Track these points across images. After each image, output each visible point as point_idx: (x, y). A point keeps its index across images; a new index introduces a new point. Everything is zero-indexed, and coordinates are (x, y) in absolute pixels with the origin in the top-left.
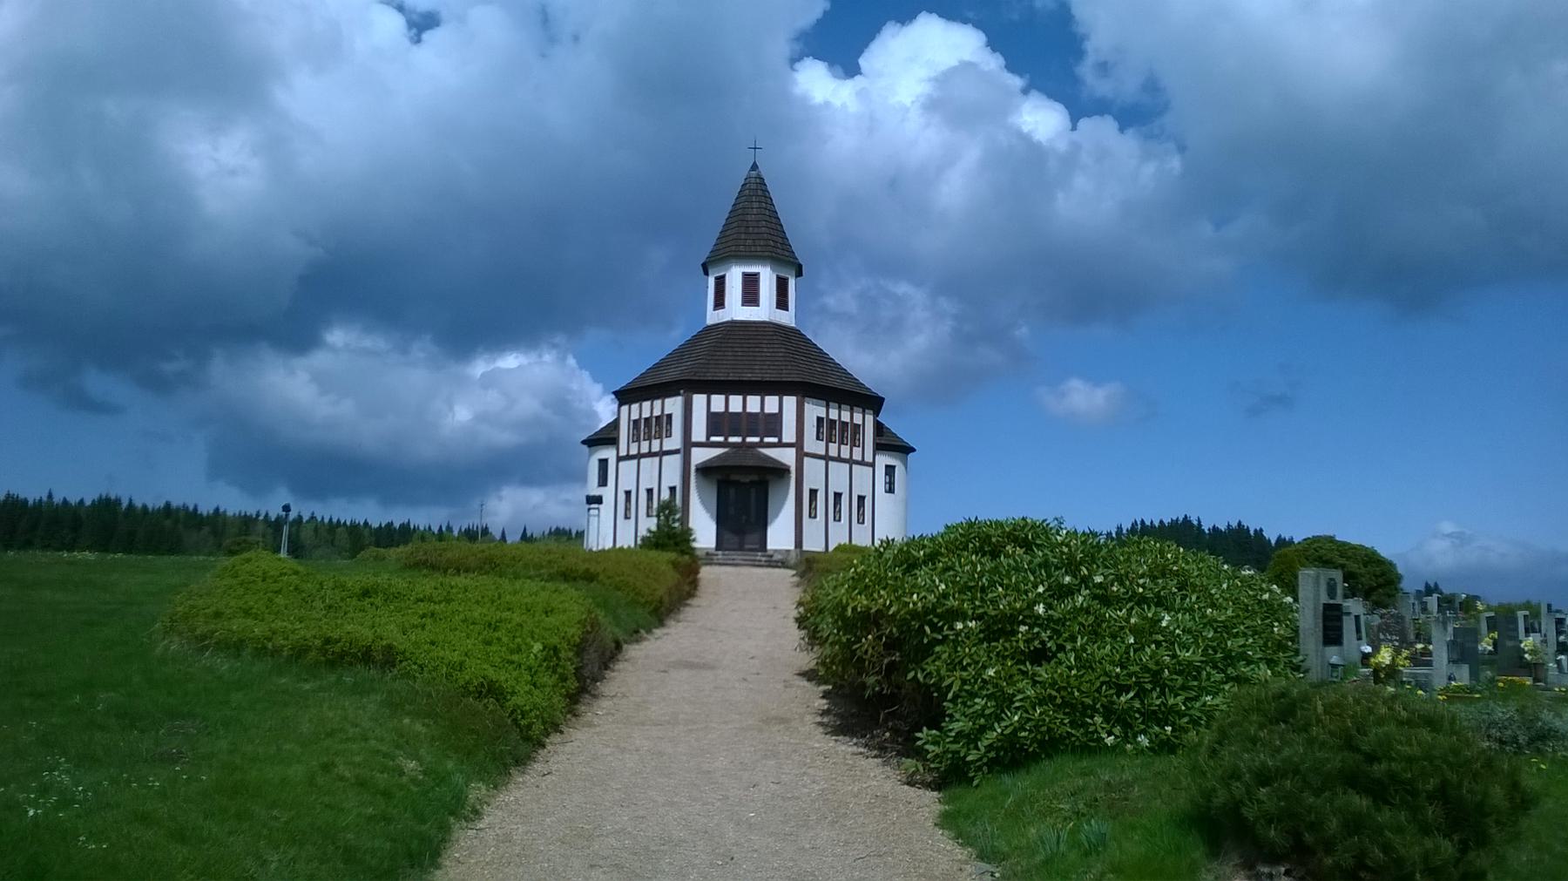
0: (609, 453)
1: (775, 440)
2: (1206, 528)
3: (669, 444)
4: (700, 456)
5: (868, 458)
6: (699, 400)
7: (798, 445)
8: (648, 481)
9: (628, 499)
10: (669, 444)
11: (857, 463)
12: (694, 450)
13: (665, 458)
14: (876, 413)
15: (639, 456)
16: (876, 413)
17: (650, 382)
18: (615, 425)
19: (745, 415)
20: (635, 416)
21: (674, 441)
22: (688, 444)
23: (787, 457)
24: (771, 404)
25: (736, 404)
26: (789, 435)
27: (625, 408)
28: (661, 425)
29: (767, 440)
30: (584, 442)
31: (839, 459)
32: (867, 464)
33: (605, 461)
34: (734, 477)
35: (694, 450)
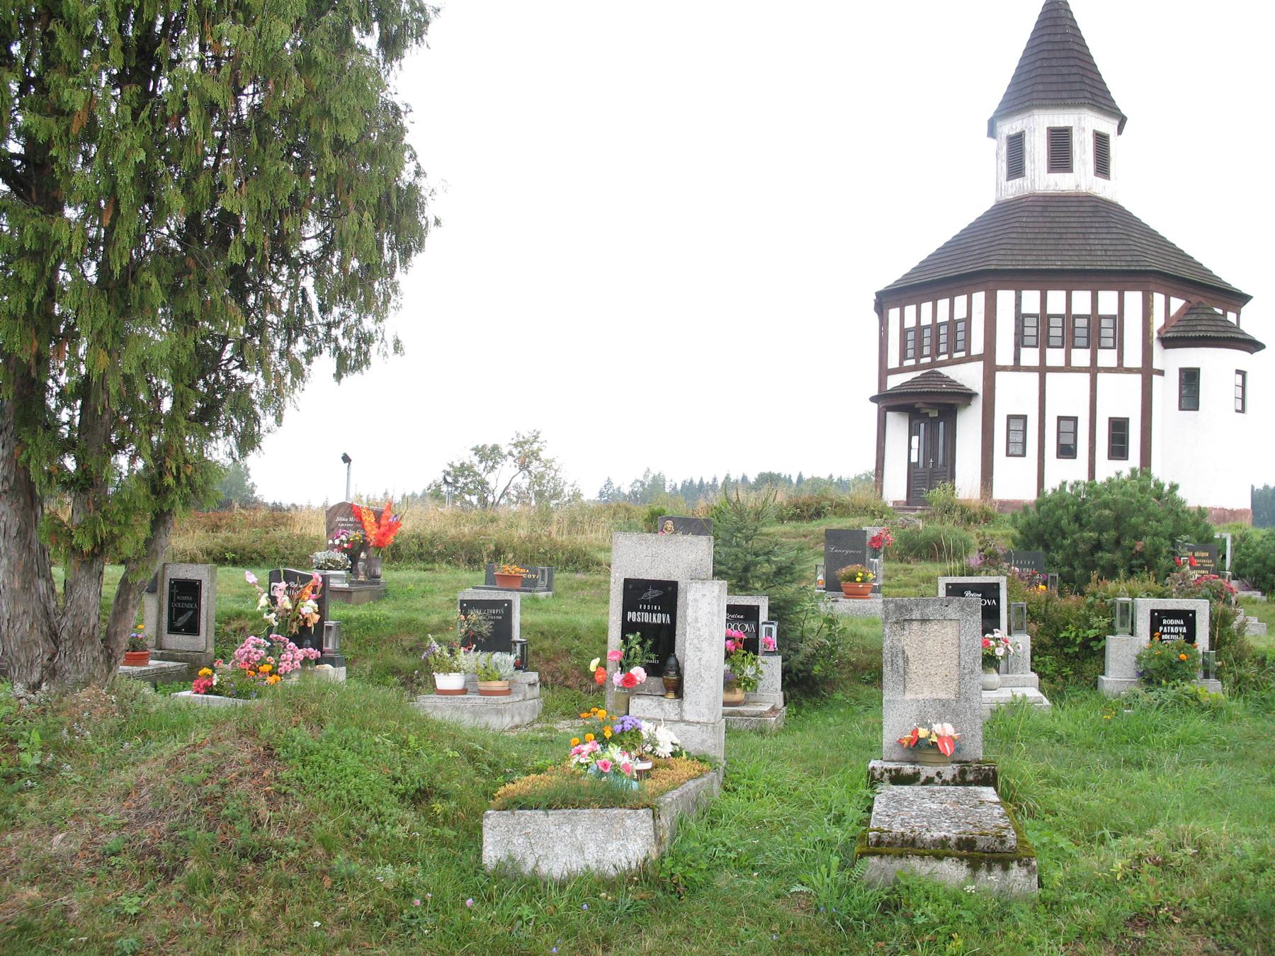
6: (1005, 298)
17: (923, 279)
24: (1108, 301)
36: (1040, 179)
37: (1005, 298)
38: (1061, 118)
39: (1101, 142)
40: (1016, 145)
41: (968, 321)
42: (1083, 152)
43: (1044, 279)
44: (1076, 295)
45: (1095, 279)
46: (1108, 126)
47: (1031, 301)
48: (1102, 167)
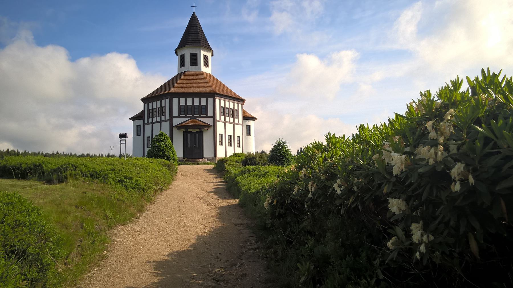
0: (140, 122)
4: (176, 122)
5: (240, 122)
6: (175, 100)
7: (214, 117)
9: (148, 141)
11: (237, 124)
12: (174, 119)
14: (242, 105)
15: (152, 123)
16: (242, 105)
18: (143, 112)
19: (193, 106)
22: (171, 117)
23: (209, 121)
24: (203, 102)
25: (189, 102)
26: (210, 113)
27: (146, 105)
28: (161, 111)
30: (130, 119)
32: (240, 125)
34: (190, 130)
37: (175, 100)
39: (206, 57)
41: (165, 106)
43: (186, 95)
45: (200, 95)
47: (182, 101)
48: (206, 64)
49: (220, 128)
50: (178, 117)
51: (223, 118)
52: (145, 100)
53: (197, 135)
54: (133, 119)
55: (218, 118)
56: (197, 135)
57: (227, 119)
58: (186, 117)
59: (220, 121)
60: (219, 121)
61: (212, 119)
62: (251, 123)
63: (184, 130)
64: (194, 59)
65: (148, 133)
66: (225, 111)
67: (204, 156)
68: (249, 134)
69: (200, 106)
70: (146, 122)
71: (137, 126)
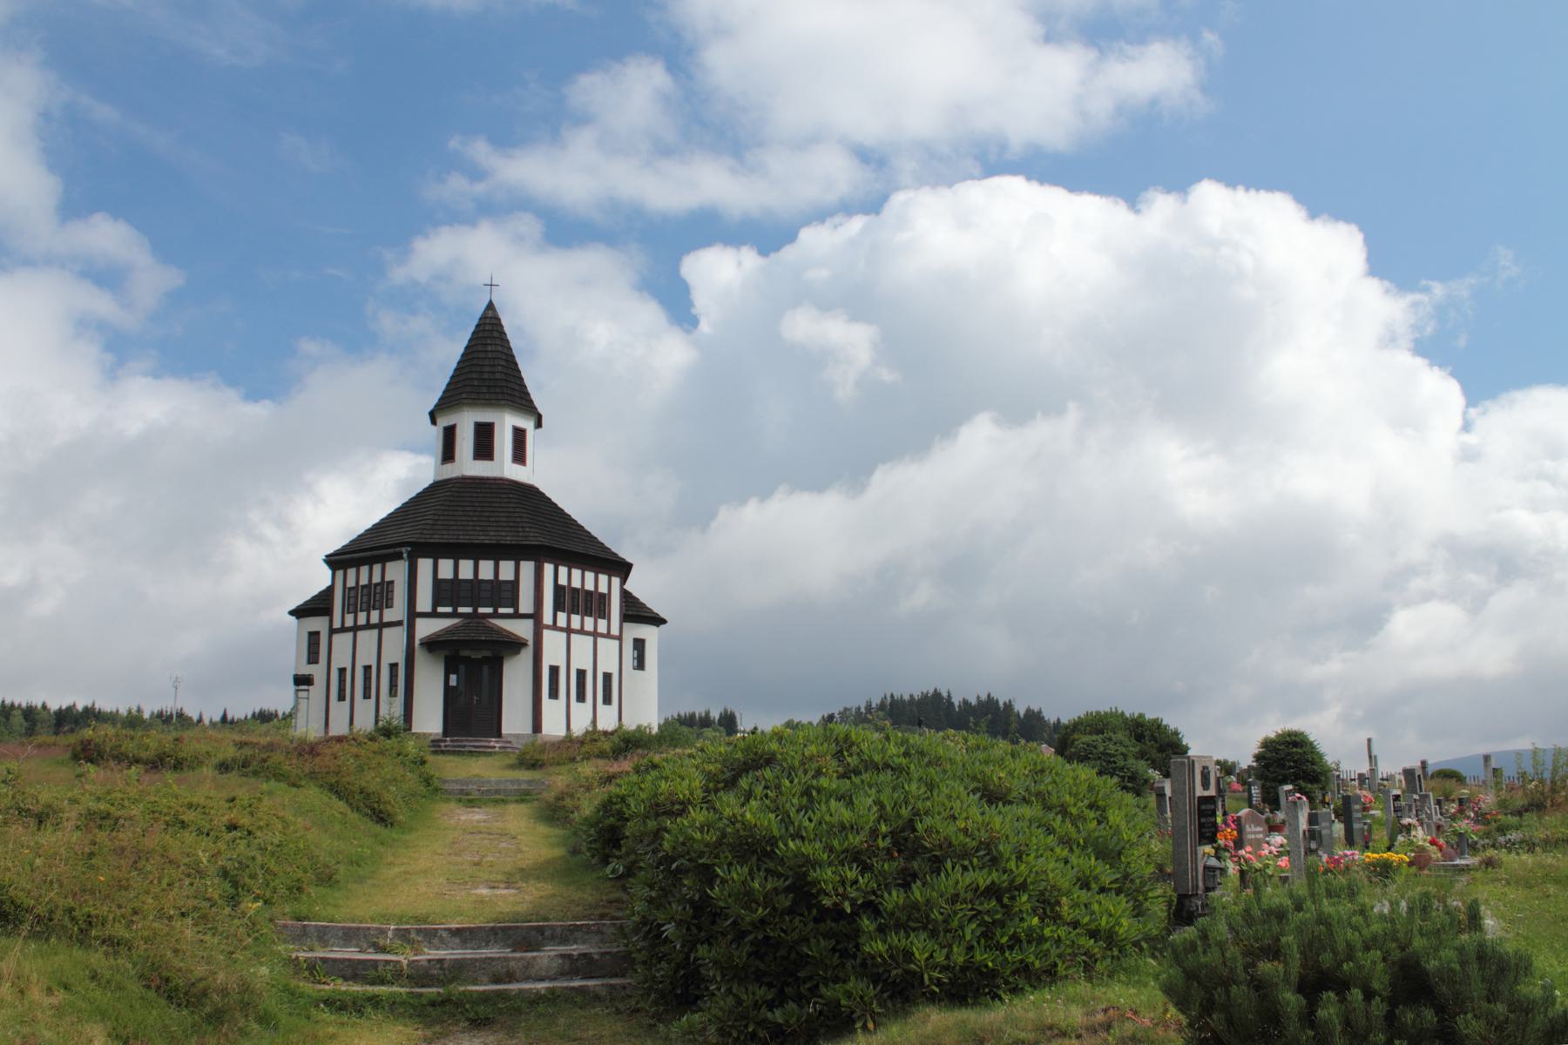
0: (318, 624)
1: (510, 610)
2: (956, 701)
3: (389, 615)
4: (425, 628)
5: (615, 631)
6: (425, 565)
7: (536, 616)
8: (366, 656)
10: (389, 615)
11: (603, 636)
12: (420, 622)
13: (386, 631)
15: (355, 629)
18: (329, 592)
19: (476, 582)
20: (351, 583)
21: (397, 612)
22: (413, 615)
23: (523, 629)
24: (507, 570)
25: (466, 570)
26: (526, 605)
27: (340, 574)
29: (501, 610)
30: (292, 613)
31: (582, 632)
32: (614, 638)
33: (317, 633)
34: (465, 653)
35: (420, 622)
36: (467, 465)
37: (425, 565)
38: (485, 416)
39: (519, 436)
40: (450, 434)
42: (503, 443)
43: (456, 551)
44: (503, 564)
45: (497, 552)
46: (527, 424)
47: (446, 569)
48: (519, 456)
49: (553, 648)
50: (434, 614)
51: (562, 618)
52: (336, 561)
53: (486, 670)
54: (300, 613)
55: (547, 618)
56: (486, 670)
57: (576, 621)
58: (454, 615)
59: (554, 627)
60: (548, 627)
61: (530, 623)
62: (648, 632)
63: (447, 653)
64: (484, 448)
65: (341, 658)
66: (568, 599)
67: (504, 732)
68: (640, 664)
69: (496, 583)
70: (337, 624)
71: (311, 634)
